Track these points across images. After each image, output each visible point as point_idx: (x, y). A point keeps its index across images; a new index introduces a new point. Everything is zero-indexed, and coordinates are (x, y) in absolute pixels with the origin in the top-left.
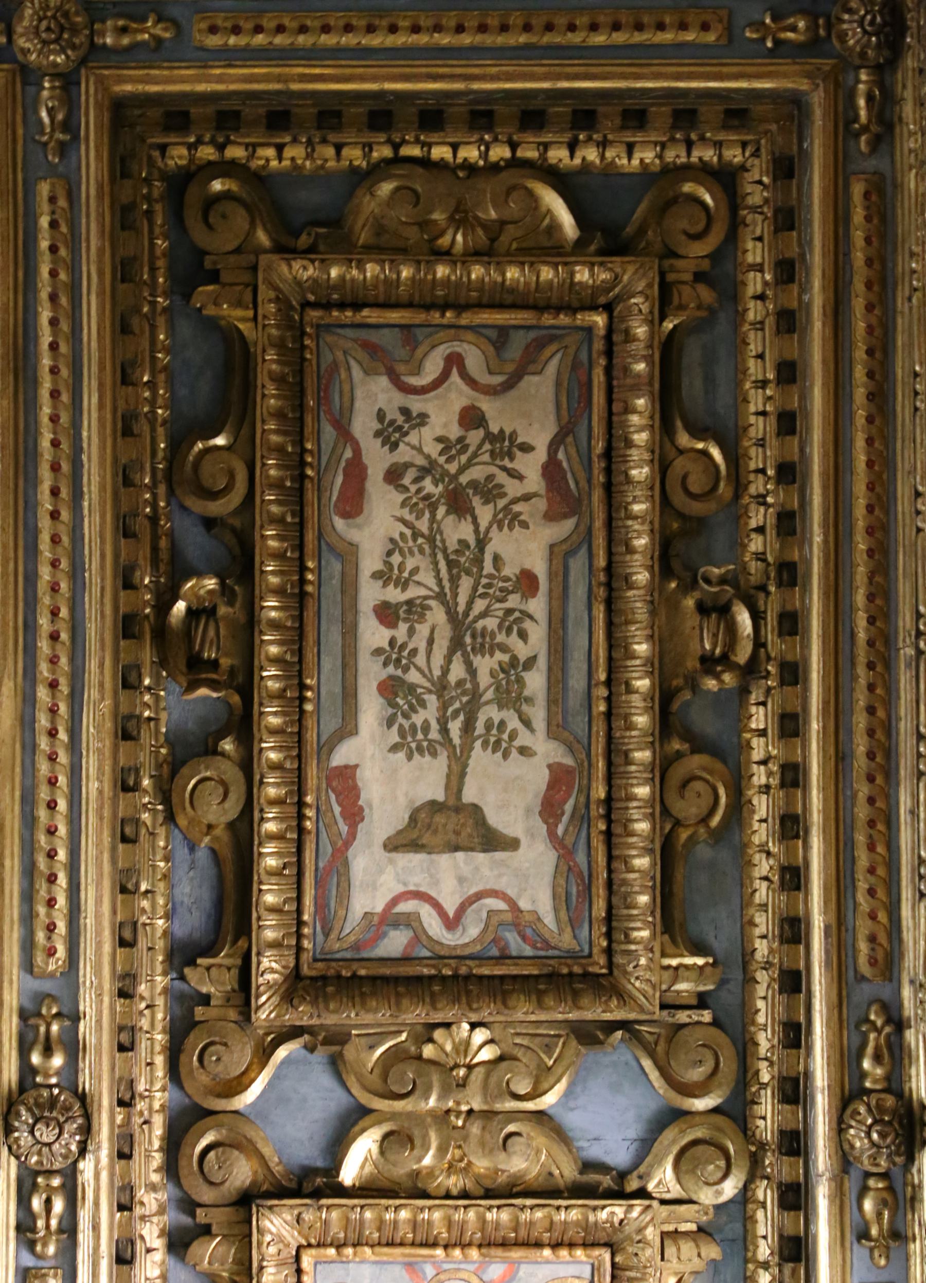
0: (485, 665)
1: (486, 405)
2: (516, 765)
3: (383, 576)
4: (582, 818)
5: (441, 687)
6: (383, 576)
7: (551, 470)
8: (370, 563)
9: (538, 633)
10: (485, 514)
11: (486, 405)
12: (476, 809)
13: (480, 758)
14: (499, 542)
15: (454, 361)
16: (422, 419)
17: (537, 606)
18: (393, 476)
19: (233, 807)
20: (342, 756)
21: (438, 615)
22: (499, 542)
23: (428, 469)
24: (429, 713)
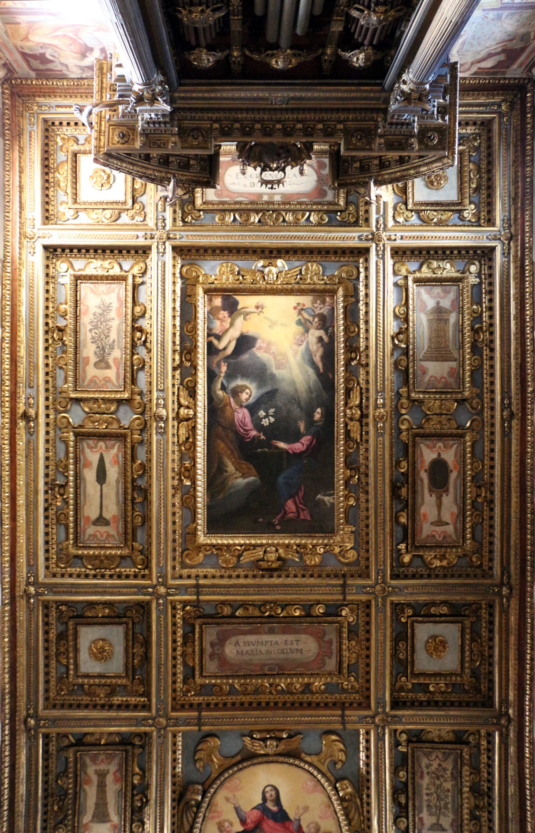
0: (442, 803)
1: (442, 763)
2: (447, 819)
3: (427, 789)
4: (457, 827)
5: (435, 806)
6: (427, 789)
7: (452, 774)
8: (425, 787)
9: (450, 798)
10: (442, 780)
11: (442, 763)
12: (441, 825)
13: (442, 817)
14: (444, 784)
15: (437, 756)
16: (432, 765)
17: (450, 794)
18: (428, 773)
19: (405, 825)
20: (421, 815)
21: (435, 795)
22: (444, 784)
23: (433, 773)
24: (434, 810)
